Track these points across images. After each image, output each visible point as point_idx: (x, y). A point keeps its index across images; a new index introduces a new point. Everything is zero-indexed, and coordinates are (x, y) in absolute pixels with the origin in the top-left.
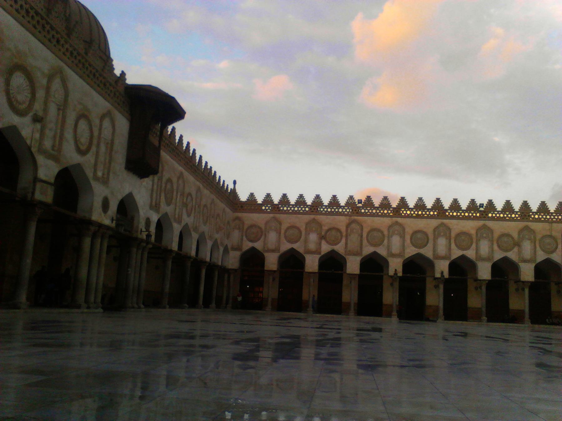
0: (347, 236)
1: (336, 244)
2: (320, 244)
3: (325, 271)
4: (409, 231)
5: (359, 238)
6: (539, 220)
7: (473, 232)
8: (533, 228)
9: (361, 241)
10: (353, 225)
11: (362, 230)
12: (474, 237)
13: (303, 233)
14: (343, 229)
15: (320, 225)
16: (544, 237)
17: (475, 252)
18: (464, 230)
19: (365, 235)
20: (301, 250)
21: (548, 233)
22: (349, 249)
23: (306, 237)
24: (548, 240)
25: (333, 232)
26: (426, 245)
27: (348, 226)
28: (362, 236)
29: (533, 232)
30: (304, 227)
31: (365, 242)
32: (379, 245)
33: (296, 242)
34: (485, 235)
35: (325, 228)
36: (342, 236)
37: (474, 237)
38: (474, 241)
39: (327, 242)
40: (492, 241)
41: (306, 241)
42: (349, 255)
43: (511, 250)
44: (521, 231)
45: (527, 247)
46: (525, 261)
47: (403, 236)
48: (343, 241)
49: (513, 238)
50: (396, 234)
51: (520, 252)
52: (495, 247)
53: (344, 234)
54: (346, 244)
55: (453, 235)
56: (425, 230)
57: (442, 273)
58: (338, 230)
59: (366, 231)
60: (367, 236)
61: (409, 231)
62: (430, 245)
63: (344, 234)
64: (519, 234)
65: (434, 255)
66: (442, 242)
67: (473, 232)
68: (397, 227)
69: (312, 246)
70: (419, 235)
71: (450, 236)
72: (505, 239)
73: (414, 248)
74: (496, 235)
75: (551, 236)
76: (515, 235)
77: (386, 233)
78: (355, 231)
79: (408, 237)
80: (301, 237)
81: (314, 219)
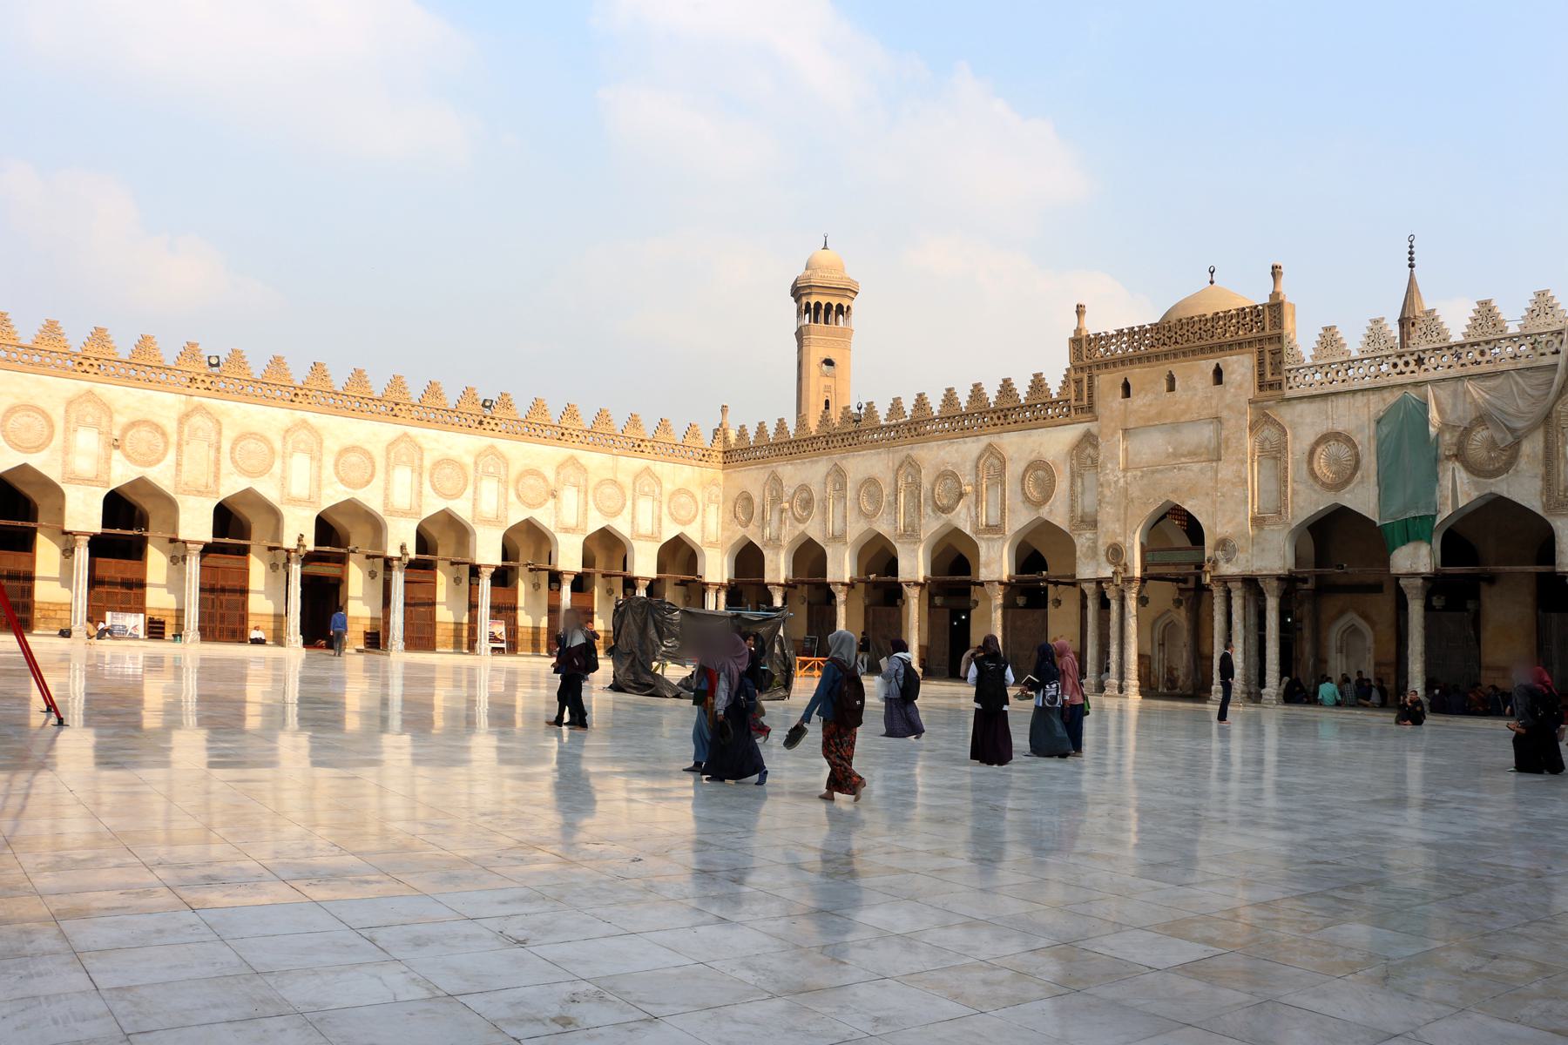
0: (179, 446)
1: (150, 464)
2: (108, 459)
3: (118, 531)
4: (332, 446)
5: (212, 453)
6: (594, 446)
7: (468, 460)
8: (582, 461)
9: (217, 462)
10: (197, 420)
11: (219, 433)
12: (471, 469)
13: (59, 426)
14: (171, 426)
15: (107, 409)
16: (601, 483)
17: (470, 504)
18: (453, 454)
19: (226, 446)
20: (53, 473)
21: (610, 476)
22: (185, 477)
23: (66, 440)
24: (609, 490)
25: (144, 433)
26: (368, 482)
27: (184, 418)
28: (218, 449)
29: (583, 469)
30: (61, 411)
31: (226, 464)
32: (261, 474)
33: (38, 448)
34: (491, 469)
35: (121, 420)
36: (166, 443)
37: (471, 469)
38: (471, 479)
39: (128, 457)
40: (504, 483)
41: (66, 450)
42: (185, 492)
43: (541, 505)
44: (561, 466)
45: (570, 497)
46: (566, 530)
47: (316, 457)
48: (171, 456)
49: (545, 479)
50: (303, 451)
51: (557, 510)
52: (512, 497)
53: (173, 438)
54: (178, 464)
55: (427, 463)
56: (368, 447)
57: (403, 548)
58: (157, 428)
59: (228, 435)
60: (233, 449)
61: (332, 446)
62: (378, 481)
63: (173, 438)
64: (558, 473)
65: (386, 505)
66: (403, 478)
67: (468, 460)
68: (303, 435)
69: (84, 464)
70: (353, 458)
71: (421, 467)
72: (531, 481)
73: (341, 487)
74: (514, 471)
75: (614, 482)
76: (551, 475)
77: (278, 445)
78: (200, 433)
79: (328, 461)
80: (50, 438)
81: (90, 392)
